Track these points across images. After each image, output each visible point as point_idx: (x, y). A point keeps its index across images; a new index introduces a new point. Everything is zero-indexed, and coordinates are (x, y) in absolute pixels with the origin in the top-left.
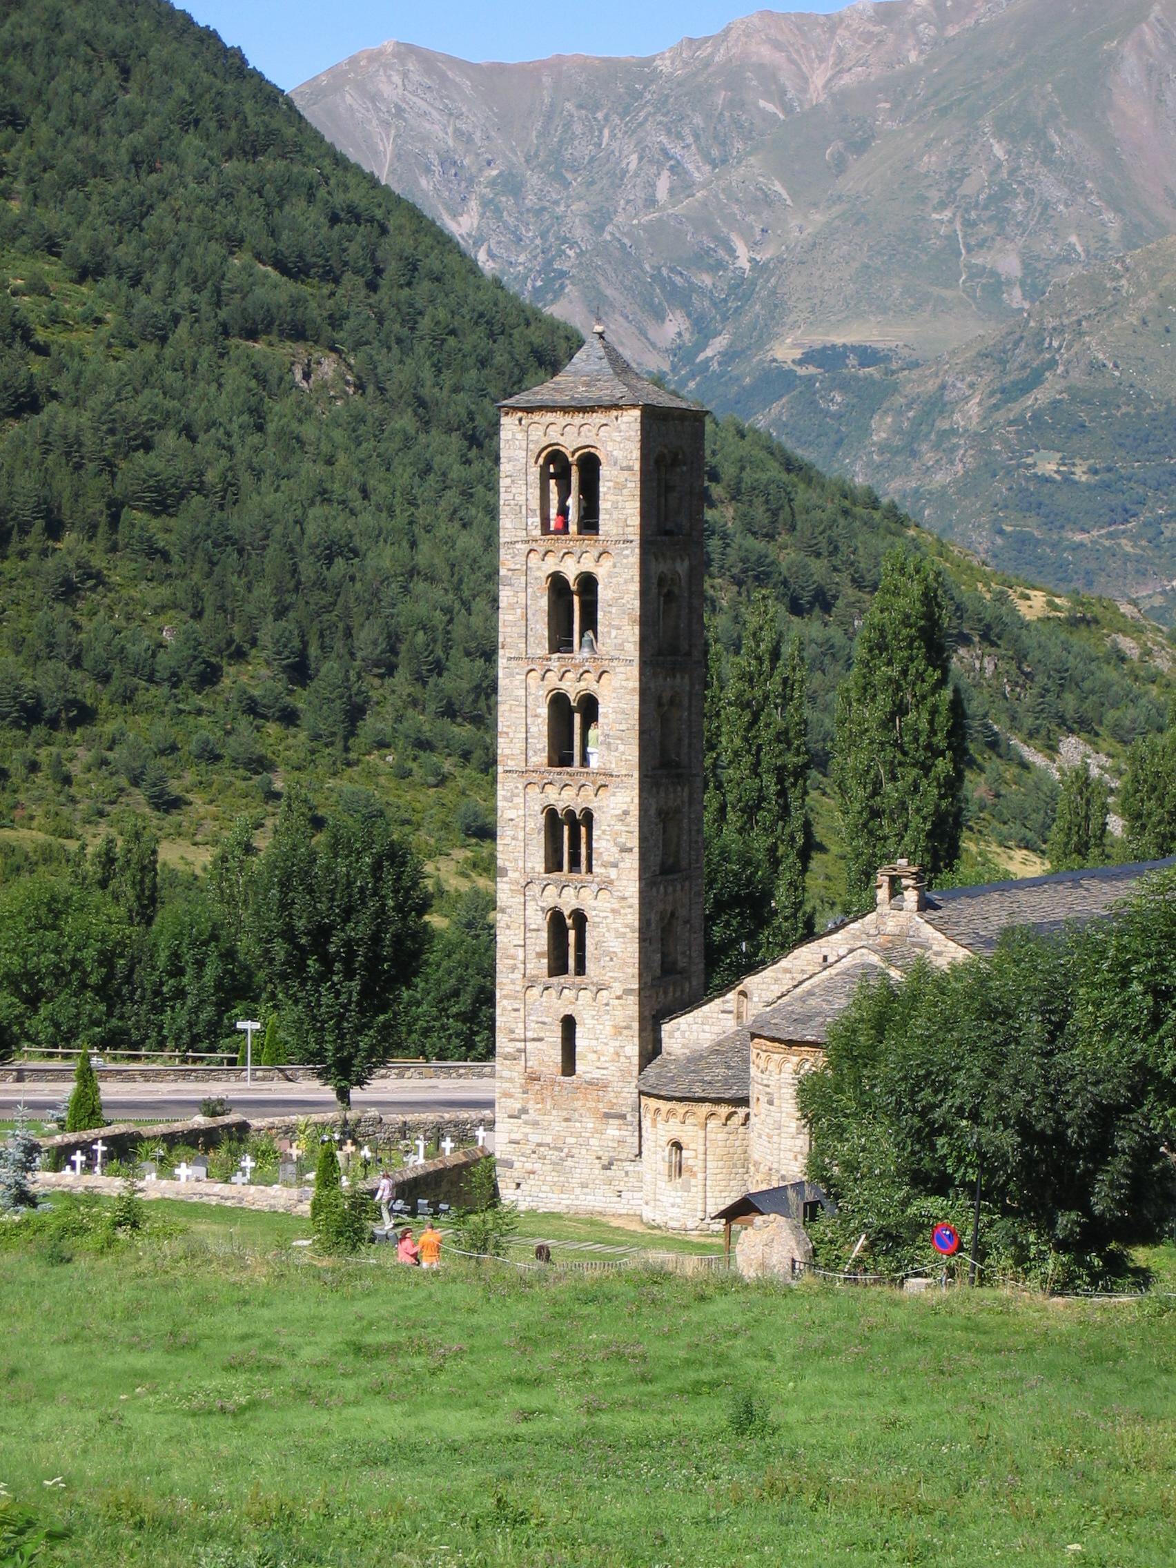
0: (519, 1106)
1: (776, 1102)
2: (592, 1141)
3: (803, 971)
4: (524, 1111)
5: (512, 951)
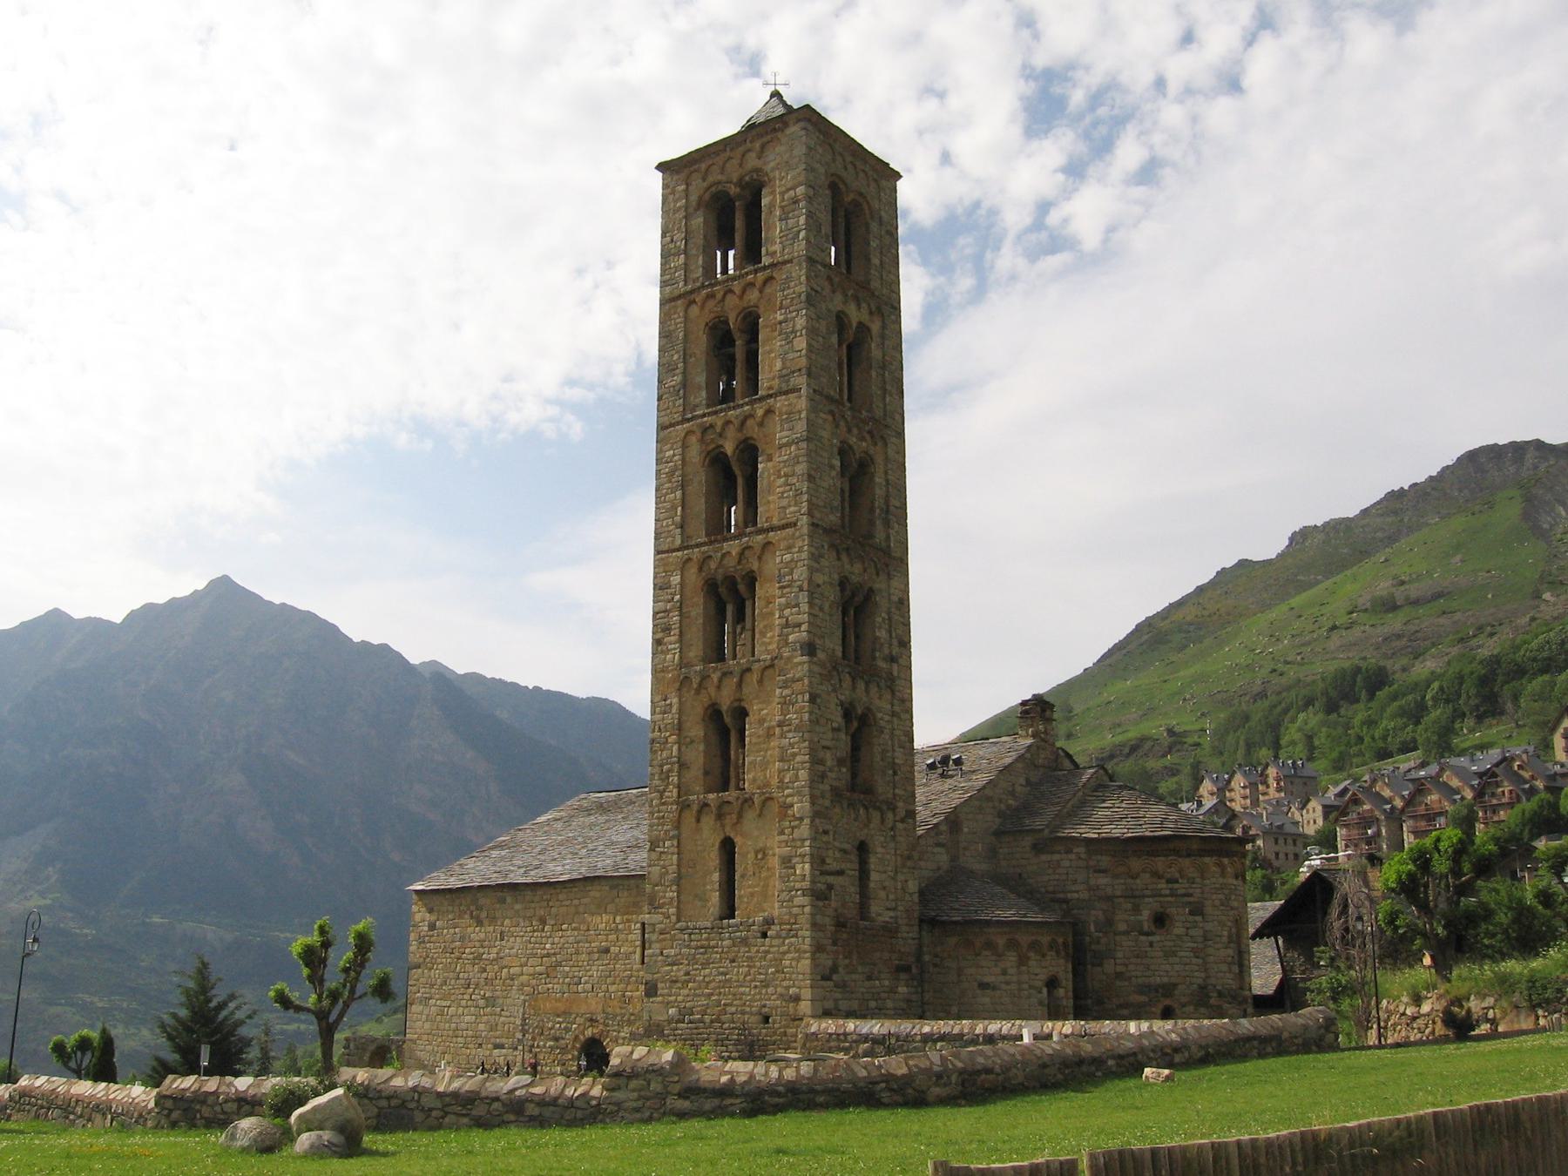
0: (830, 963)
1: (1208, 910)
2: (889, 1004)
3: (1000, 801)
4: (834, 969)
5: (821, 754)
